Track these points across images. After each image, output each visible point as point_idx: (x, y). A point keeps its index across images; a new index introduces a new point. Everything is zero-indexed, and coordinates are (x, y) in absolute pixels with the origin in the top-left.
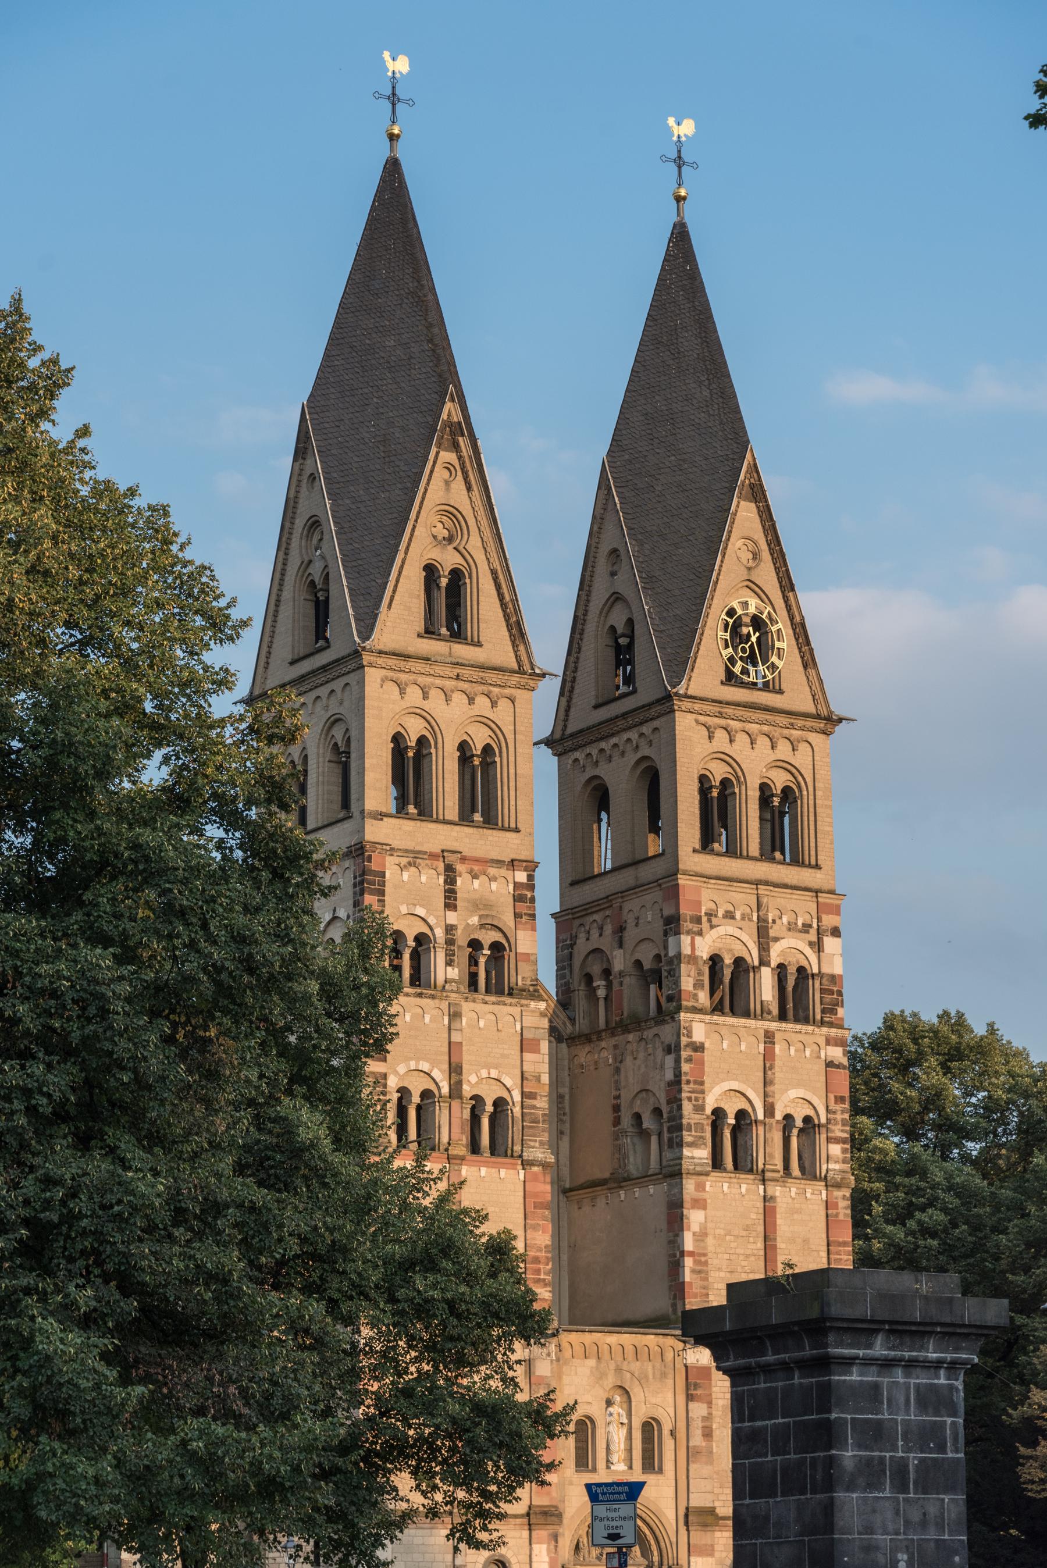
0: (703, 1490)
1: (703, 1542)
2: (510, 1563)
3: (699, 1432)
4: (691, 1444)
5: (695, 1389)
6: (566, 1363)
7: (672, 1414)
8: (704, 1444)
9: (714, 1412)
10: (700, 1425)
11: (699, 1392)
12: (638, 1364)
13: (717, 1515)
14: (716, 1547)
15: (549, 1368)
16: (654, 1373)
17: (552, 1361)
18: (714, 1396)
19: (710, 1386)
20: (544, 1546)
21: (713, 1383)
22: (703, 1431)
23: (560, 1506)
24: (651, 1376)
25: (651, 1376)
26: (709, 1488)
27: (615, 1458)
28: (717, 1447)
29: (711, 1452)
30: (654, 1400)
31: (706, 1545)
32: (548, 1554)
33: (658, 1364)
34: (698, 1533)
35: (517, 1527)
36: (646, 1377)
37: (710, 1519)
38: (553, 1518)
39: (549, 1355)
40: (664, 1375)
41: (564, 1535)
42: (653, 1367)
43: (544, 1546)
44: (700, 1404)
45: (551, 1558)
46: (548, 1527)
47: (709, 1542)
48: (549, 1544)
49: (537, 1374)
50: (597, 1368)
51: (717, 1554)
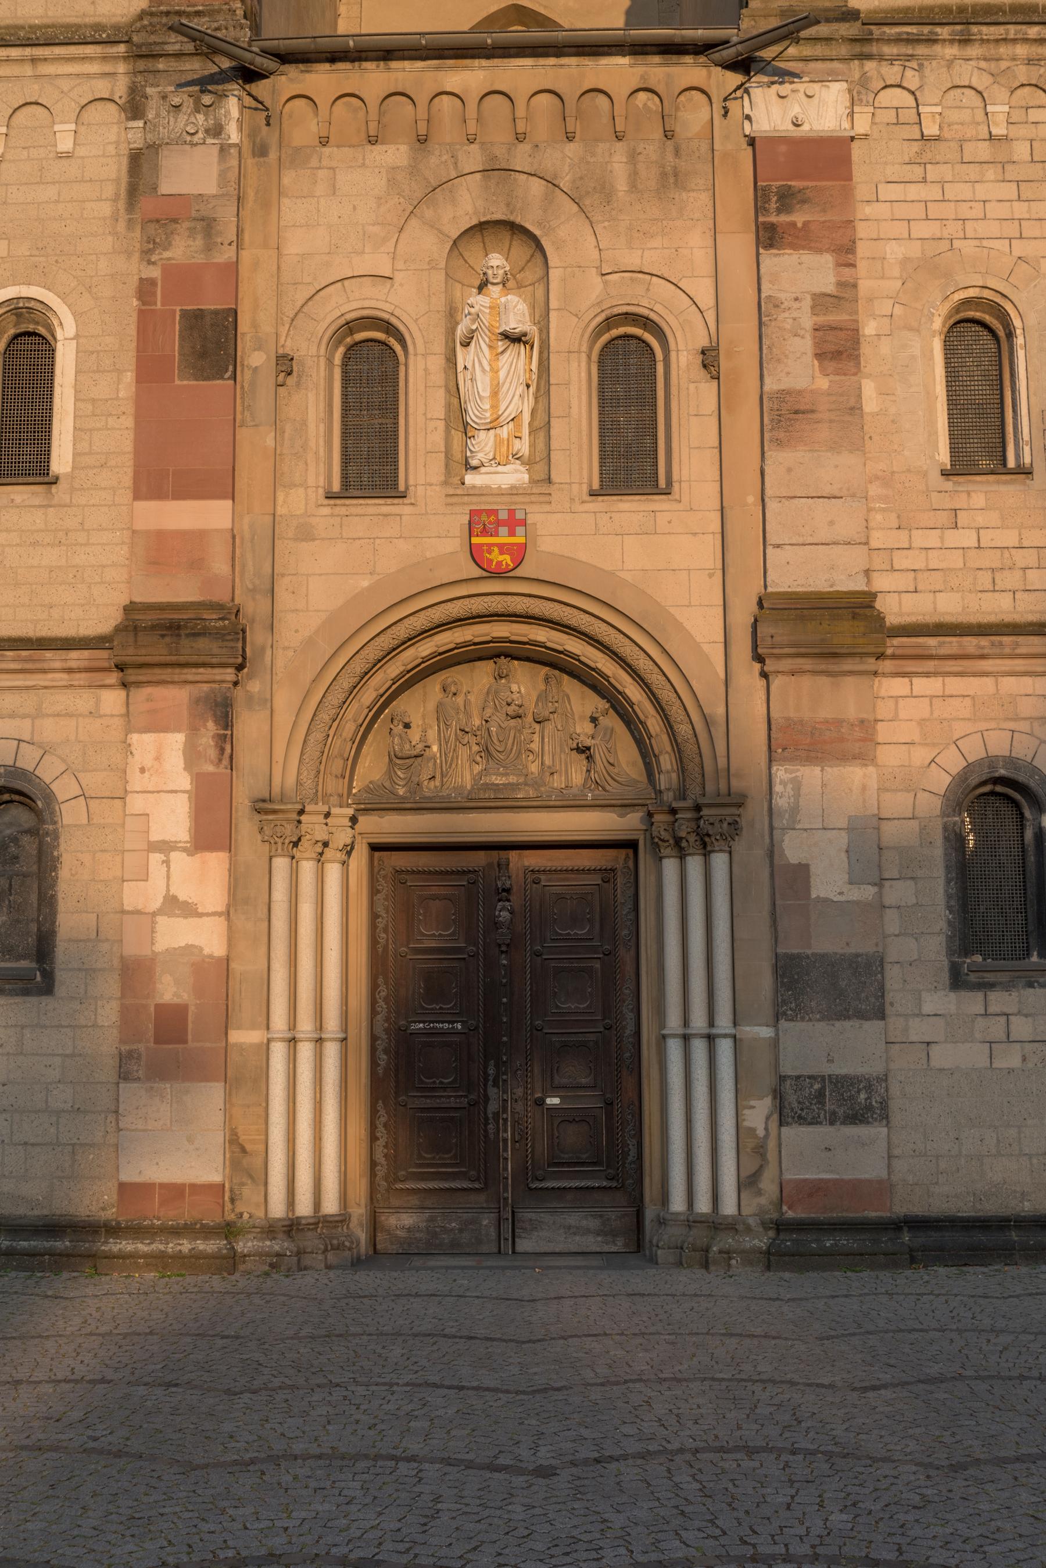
0: (823, 535)
1: (825, 712)
2: (49, 797)
3: (805, 345)
4: (770, 385)
6: (298, 157)
7: (706, 299)
8: (823, 383)
9: (865, 286)
10: (807, 321)
11: (798, 218)
13: (880, 618)
14: (883, 733)
15: (215, 170)
16: (633, 178)
17: (223, 149)
18: (863, 230)
19: (847, 194)
20: (176, 740)
21: (862, 190)
22: (816, 345)
23: (253, 607)
24: (621, 185)
25: (621, 185)
26: (848, 526)
27: (483, 446)
28: (883, 393)
29: (855, 409)
30: (633, 259)
31: (839, 723)
32: (188, 766)
33: (651, 147)
34: (806, 682)
35: (81, 678)
36: (606, 192)
37: (845, 632)
38: (202, 643)
39: (217, 130)
41: (268, 702)
42: (633, 157)
43: (176, 740)
44: (808, 258)
45: (200, 781)
46: (190, 674)
47: (852, 712)
48: (193, 731)
49: (165, 188)
50: (413, 170)
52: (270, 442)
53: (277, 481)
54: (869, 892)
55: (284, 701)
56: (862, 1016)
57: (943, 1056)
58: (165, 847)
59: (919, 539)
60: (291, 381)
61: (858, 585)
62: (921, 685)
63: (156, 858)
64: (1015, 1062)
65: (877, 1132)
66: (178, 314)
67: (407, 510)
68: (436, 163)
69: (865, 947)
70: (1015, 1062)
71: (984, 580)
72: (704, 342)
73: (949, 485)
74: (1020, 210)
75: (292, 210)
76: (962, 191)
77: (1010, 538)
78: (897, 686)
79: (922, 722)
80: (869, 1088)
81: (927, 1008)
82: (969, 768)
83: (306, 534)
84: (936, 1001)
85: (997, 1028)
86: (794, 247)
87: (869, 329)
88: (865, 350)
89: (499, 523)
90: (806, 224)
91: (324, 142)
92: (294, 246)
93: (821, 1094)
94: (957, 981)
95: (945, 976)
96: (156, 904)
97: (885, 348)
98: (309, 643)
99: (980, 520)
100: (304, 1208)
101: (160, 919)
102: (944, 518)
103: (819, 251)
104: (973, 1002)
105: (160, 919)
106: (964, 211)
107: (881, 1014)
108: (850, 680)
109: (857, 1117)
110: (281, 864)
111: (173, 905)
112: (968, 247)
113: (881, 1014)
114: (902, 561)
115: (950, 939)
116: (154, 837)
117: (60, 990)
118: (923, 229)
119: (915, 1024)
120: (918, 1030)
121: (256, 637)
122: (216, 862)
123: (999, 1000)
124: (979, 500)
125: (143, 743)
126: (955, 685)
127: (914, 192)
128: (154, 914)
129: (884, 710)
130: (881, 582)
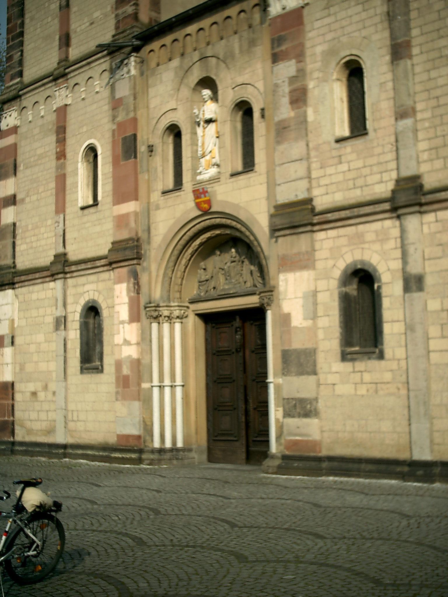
0: (294, 177)
1: (295, 251)
3: (286, 100)
5: (279, 45)
8: (292, 114)
11: (283, 48)
12: (223, 41)
18: (308, 44)
20: (124, 286)
21: (308, 27)
24: (237, 51)
25: (237, 51)
28: (316, 112)
29: (305, 121)
31: (299, 254)
40: (252, 43)
43: (124, 286)
44: (287, 64)
45: (131, 299)
48: (128, 282)
51: (319, 265)
52: (147, 177)
53: (149, 191)
54: (309, 323)
55: (154, 267)
56: (308, 374)
57: (340, 389)
58: (123, 322)
59: (330, 170)
60: (153, 153)
61: (302, 196)
62: (332, 233)
63: (121, 326)
64: (364, 392)
65: (315, 421)
66: (121, 139)
67: (182, 193)
68: (187, 62)
69: (309, 345)
70: (364, 392)
71: (351, 183)
72: (262, 106)
73: (338, 145)
74: (364, 15)
75: (152, 92)
76: (343, 14)
77: (360, 164)
78: (321, 235)
79: (331, 249)
80: (311, 403)
81: (334, 369)
82: (347, 267)
83: (158, 208)
84: (339, 366)
85: (357, 377)
86: (282, 60)
87: (311, 85)
88: (310, 95)
89: (201, 193)
90: (286, 49)
91: (158, 65)
92: (152, 106)
93: (295, 406)
94: (344, 357)
95: (339, 356)
96: (121, 342)
97: (316, 92)
98: (160, 246)
99: (350, 157)
100: (168, 444)
101: (123, 347)
102: (336, 160)
103: (290, 59)
104: (348, 366)
105: (123, 347)
106: (344, 23)
107: (315, 373)
108: (303, 236)
109: (307, 415)
110: (155, 325)
111: (127, 342)
112: (344, 39)
113: (315, 373)
114: (323, 182)
115: (341, 340)
116: (121, 319)
117: (105, 371)
118: (329, 37)
119: (329, 376)
120: (331, 378)
121: (145, 246)
122: (135, 325)
123: (360, 365)
124: (349, 150)
125: (118, 287)
126: (342, 231)
127: (327, 21)
128: (121, 345)
129: (317, 246)
130: (316, 192)
